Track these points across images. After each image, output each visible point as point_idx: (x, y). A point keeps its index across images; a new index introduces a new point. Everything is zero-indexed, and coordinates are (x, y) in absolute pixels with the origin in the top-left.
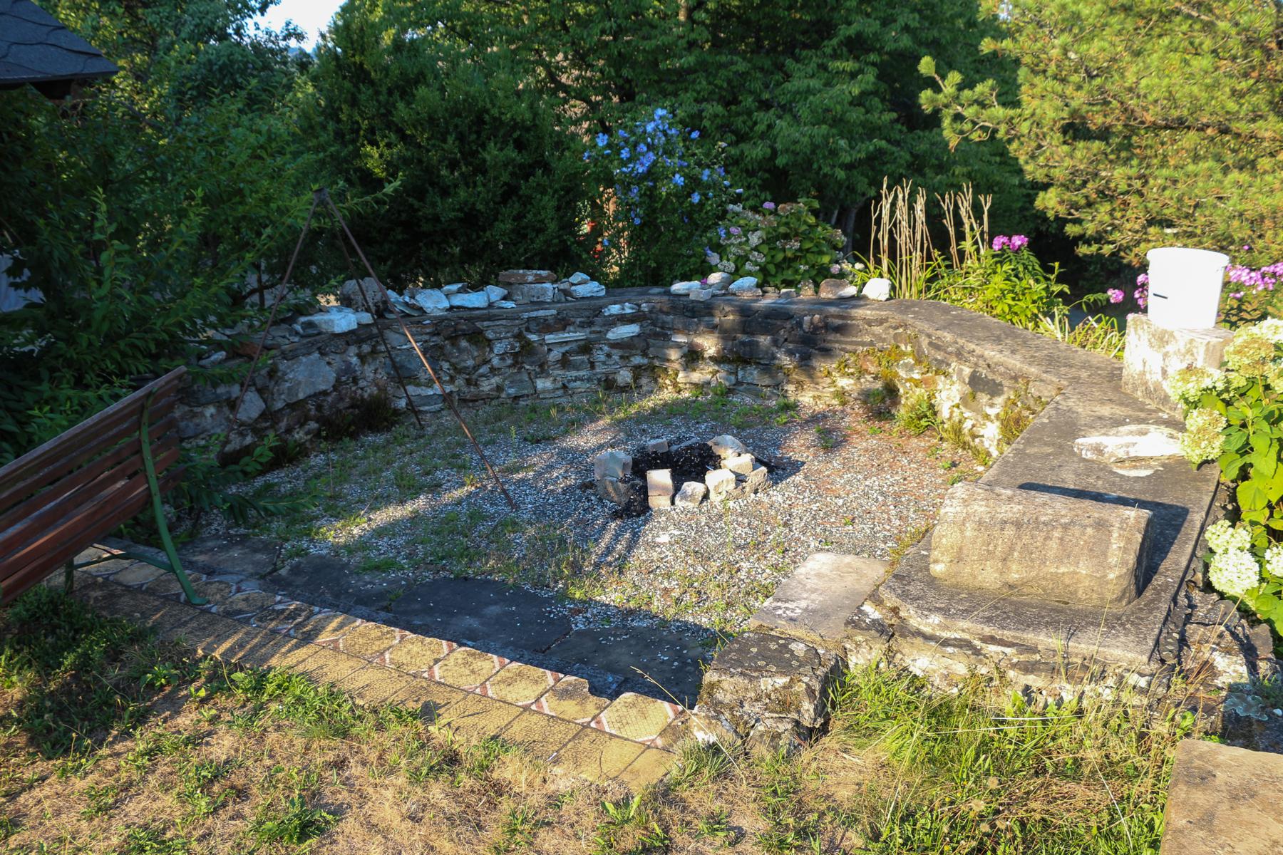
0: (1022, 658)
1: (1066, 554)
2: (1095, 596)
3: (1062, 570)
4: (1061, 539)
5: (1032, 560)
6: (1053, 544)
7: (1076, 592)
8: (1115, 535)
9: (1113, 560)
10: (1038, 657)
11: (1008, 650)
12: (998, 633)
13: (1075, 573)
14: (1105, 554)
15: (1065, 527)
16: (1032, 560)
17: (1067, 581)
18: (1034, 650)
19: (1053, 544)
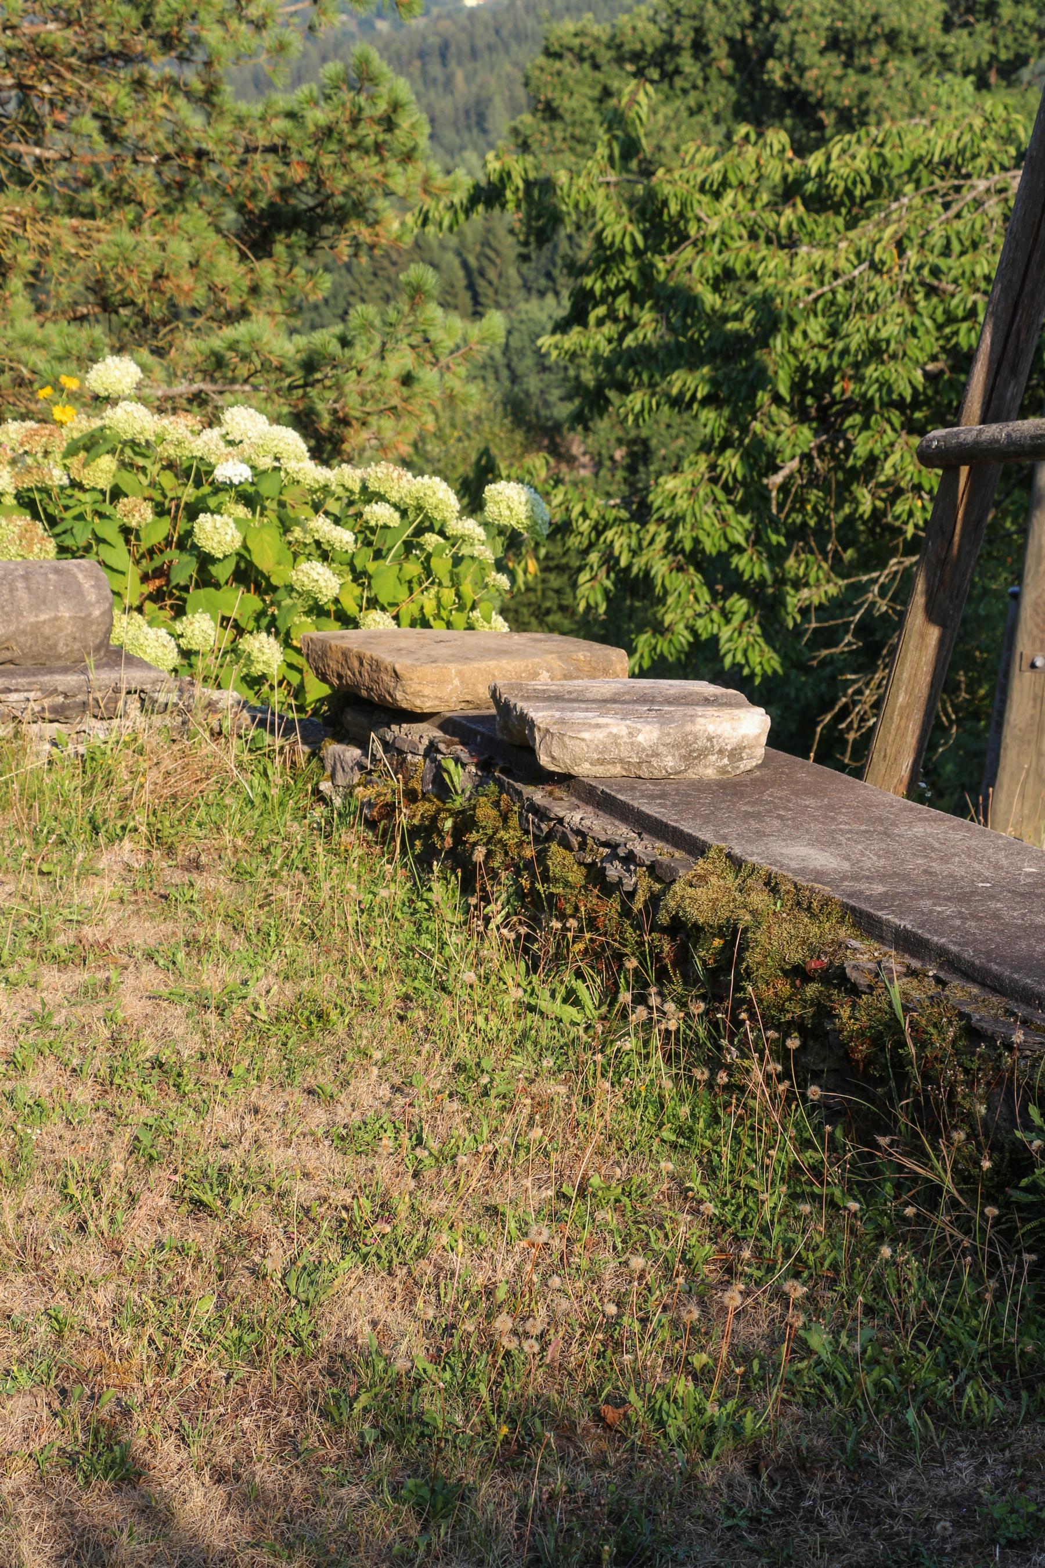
0: (47, 703)
1: (40, 602)
2: (77, 645)
3: (43, 617)
4: (28, 588)
5: (7, 614)
6: (22, 594)
7: (56, 645)
8: (80, 576)
9: (92, 597)
10: (61, 699)
11: (32, 695)
12: (13, 683)
13: (56, 619)
14: (80, 593)
15: (26, 577)
16: (7, 614)
17: (47, 630)
18: (55, 692)
19: (22, 594)
